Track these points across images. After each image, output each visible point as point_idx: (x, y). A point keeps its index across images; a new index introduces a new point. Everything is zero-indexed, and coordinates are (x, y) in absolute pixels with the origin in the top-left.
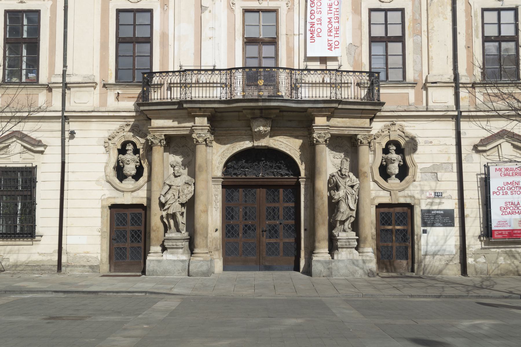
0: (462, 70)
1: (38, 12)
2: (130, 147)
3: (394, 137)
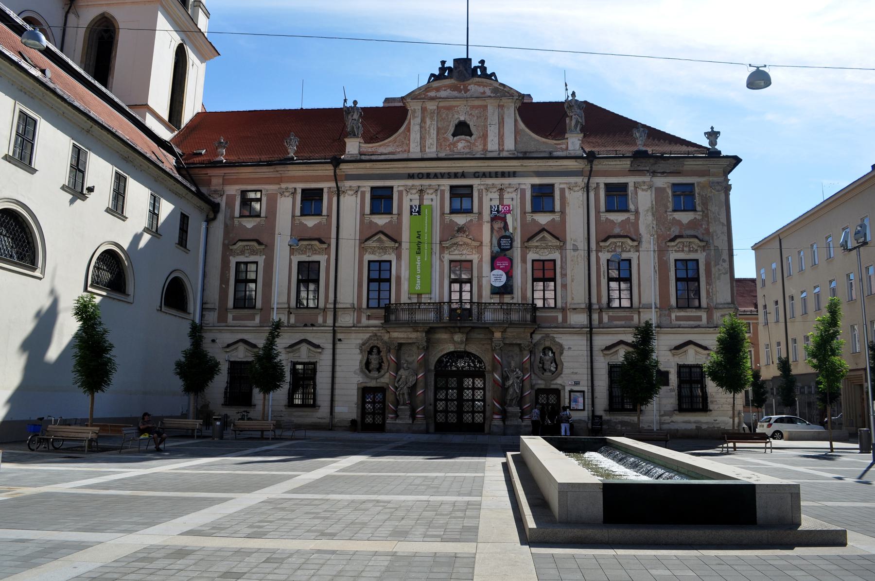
0: (594, 300)
1: (319, 262)
2: (375, 350)
3: (548, 344)
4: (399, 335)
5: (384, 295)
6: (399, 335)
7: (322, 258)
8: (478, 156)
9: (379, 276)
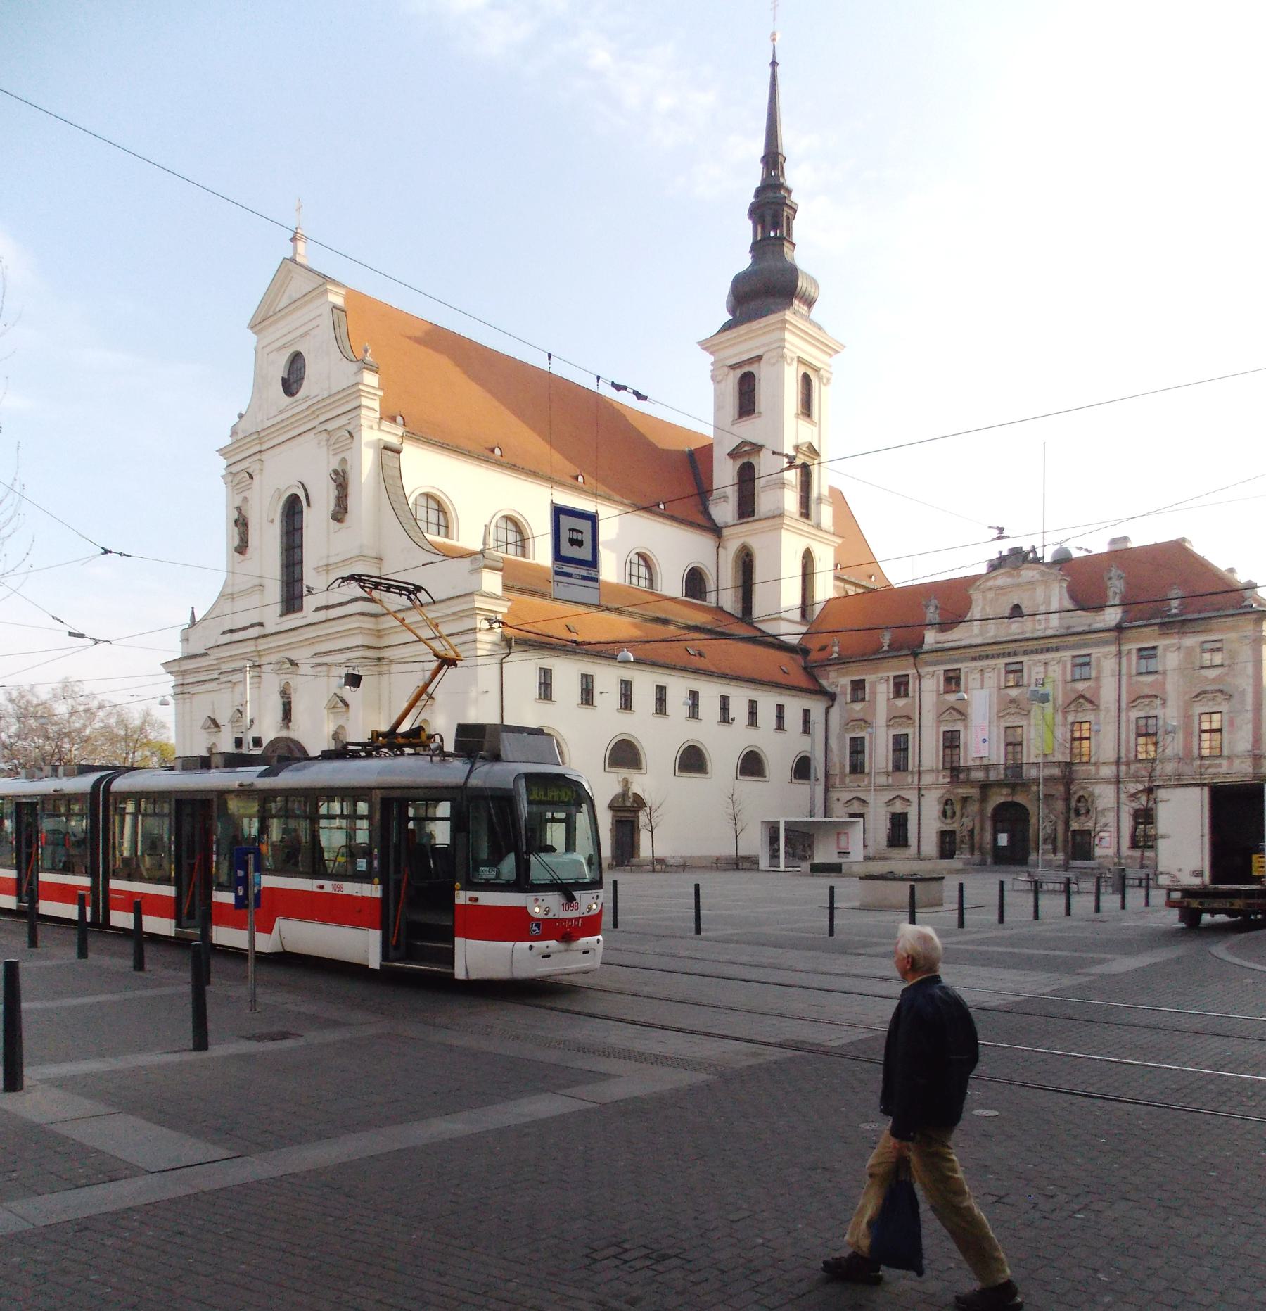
0: (1123, 754)
4: (963, 791)
5: (955, 758)
6: (963, 791)
7: (909, 731)
8: (1028, 635)
9: (951, 742)
